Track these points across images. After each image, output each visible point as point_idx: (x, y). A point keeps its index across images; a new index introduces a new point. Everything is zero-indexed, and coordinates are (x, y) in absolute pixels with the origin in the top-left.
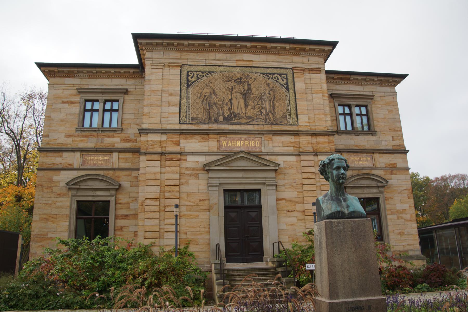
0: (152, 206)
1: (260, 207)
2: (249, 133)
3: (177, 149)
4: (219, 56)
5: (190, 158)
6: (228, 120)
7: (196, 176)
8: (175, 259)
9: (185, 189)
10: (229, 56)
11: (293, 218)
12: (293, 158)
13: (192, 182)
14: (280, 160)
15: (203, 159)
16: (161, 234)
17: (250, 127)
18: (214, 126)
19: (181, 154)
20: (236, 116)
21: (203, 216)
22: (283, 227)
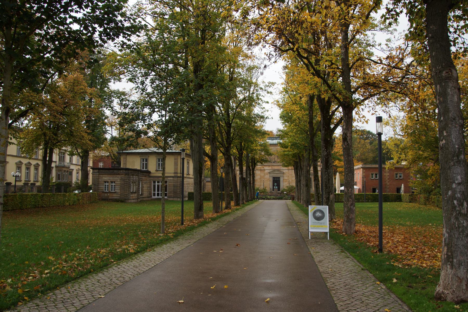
0: (259, 180)
1: (280, 181)
2: (278, 165)
3: (263, 169)
4: (272, 147)
5: (266, 171)
6: (274, 162)
7: (267, 174)
8: (263, 190)
9: (265, 177)
10: (275, 147)
11: (286, 183)
12: (287, 171)
13: (266, 175)
14: (284, 171)
15: (269, 171)
16: (261, 185)
17: (278, 164)
18: (271, 164)
19: (264, 170)
20: (276, 161)
21: (269, 182)
22: (284, 185)
